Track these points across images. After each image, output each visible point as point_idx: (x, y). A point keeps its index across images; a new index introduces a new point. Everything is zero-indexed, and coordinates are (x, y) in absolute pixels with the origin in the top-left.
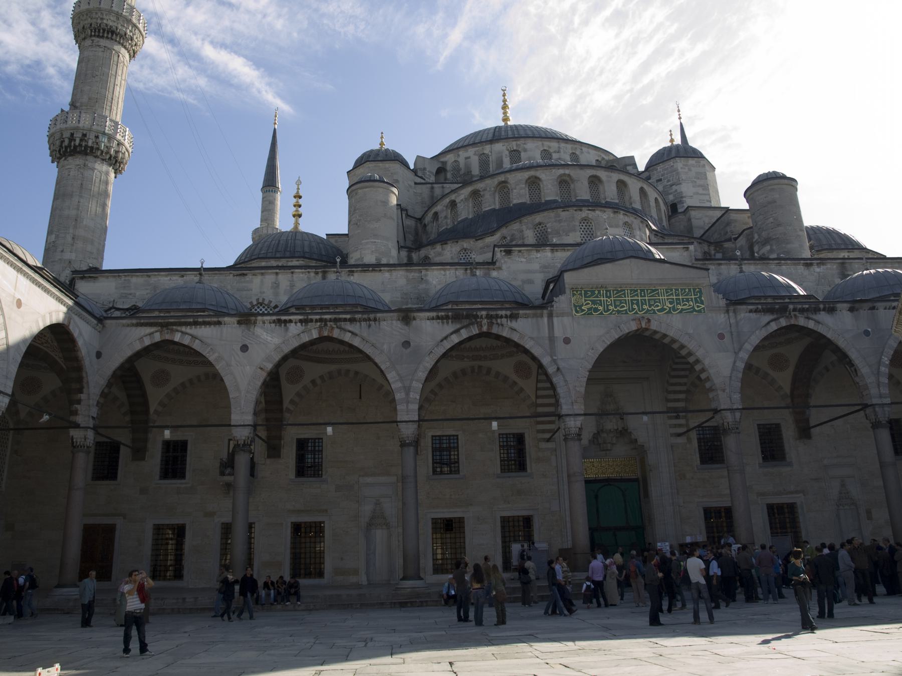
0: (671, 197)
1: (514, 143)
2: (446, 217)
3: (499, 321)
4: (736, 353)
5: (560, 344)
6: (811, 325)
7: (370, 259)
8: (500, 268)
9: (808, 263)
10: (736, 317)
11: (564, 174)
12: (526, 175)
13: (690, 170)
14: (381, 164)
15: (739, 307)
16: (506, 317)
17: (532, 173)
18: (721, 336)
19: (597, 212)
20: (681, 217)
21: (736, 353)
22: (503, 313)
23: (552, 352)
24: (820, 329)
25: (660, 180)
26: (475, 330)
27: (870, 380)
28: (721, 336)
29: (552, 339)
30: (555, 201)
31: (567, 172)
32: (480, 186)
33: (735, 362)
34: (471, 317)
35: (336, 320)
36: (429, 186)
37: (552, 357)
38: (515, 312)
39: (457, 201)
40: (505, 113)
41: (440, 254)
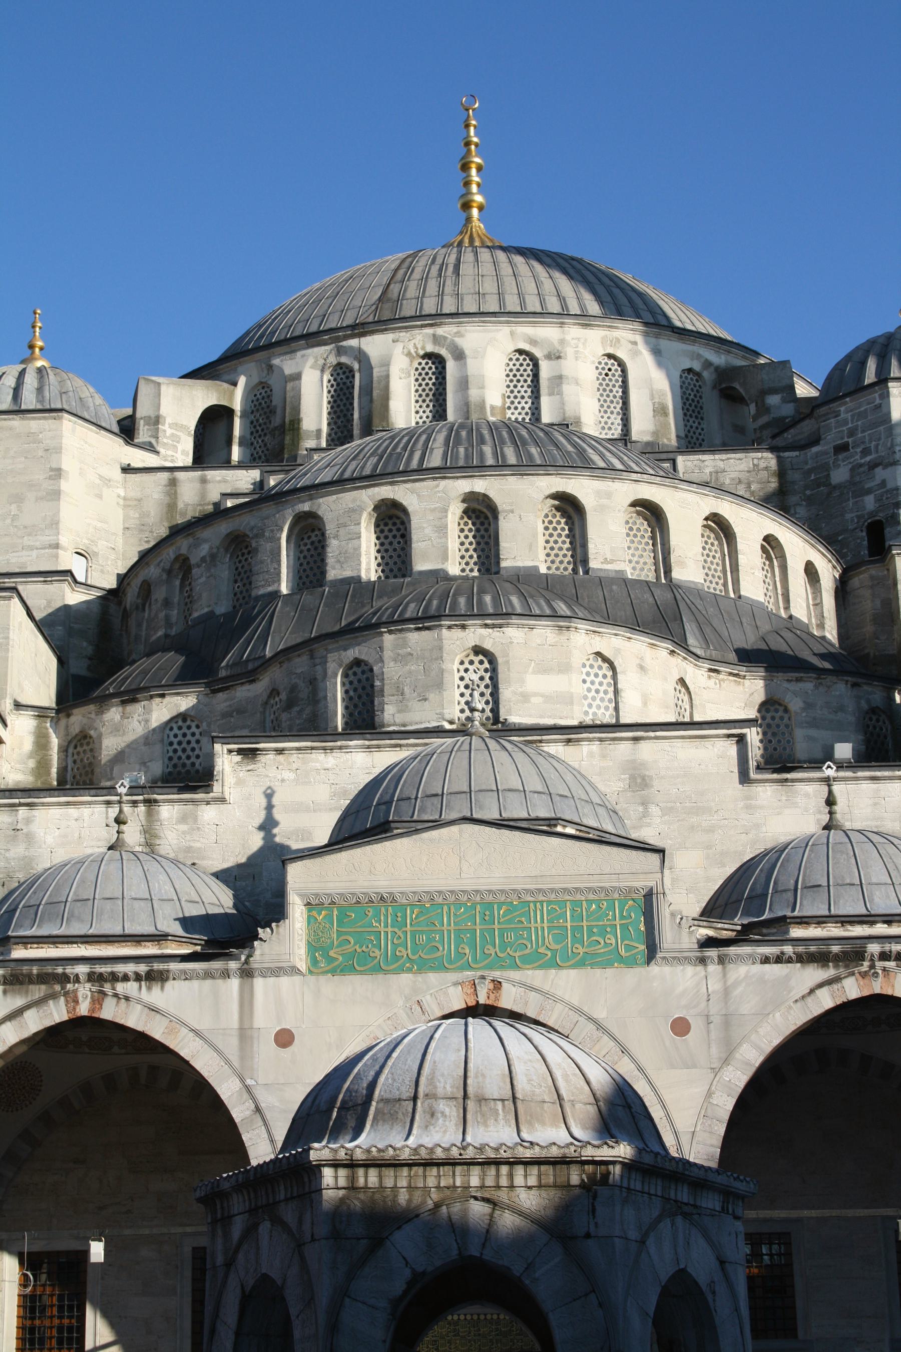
0: (869, 502)
1: (429, 331)
2: (167, 603)
3: (120, 987)
4: (716, 1071)
5: (266, 1047)
8: (222, 800)
10: (725, 975)
12: (367, 498)
14: (16, 422)
15: (732, 950)
16: (138, 978)
17: (385, 492)
18: (681, 1027)
19: (510, 632)
20: (874, 570)
22: (129, 968)
25: (842, 448)
26: (57, 1013)
28: (681, 1027)
29: (245, 1034)
30: (439, 576)
31: (479, 485)
33: (709, 1094)
34: (51, 978)
36: (165, 475)
37: (242, 1081)
38: (157, 966)
39: (193, 560)
40: (467, 184)
41: (117, 729)
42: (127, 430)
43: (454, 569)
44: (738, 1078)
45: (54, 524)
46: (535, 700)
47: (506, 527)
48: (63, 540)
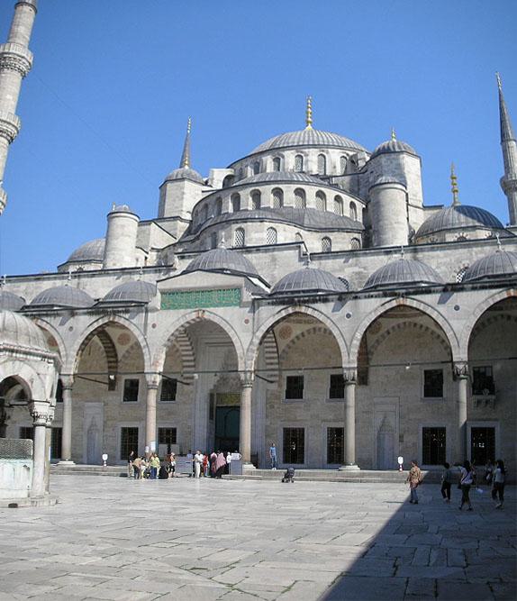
5: (150, 327)
6: (309, 311)
7: (110, 266)
9: (388, 252)
11: (255, 190)
13: (391, 162)
16: (123, 312)
19: (249, 224)
21: (254, 333)
22: (120, 309)
23: (145, 334)
24: (316, 314)
26: (107, 321)
27: (343, 350)
28: (247, 321)
29: (146, 325)
30: (247, 210)
32: (208, 201)
35: (39, 315)
42: (206, 184)
43: (250, 208)
44: (260, 334)
45: (182, 205)
46: (254, 240)
47: (262, 196)
48: (184, 209)
